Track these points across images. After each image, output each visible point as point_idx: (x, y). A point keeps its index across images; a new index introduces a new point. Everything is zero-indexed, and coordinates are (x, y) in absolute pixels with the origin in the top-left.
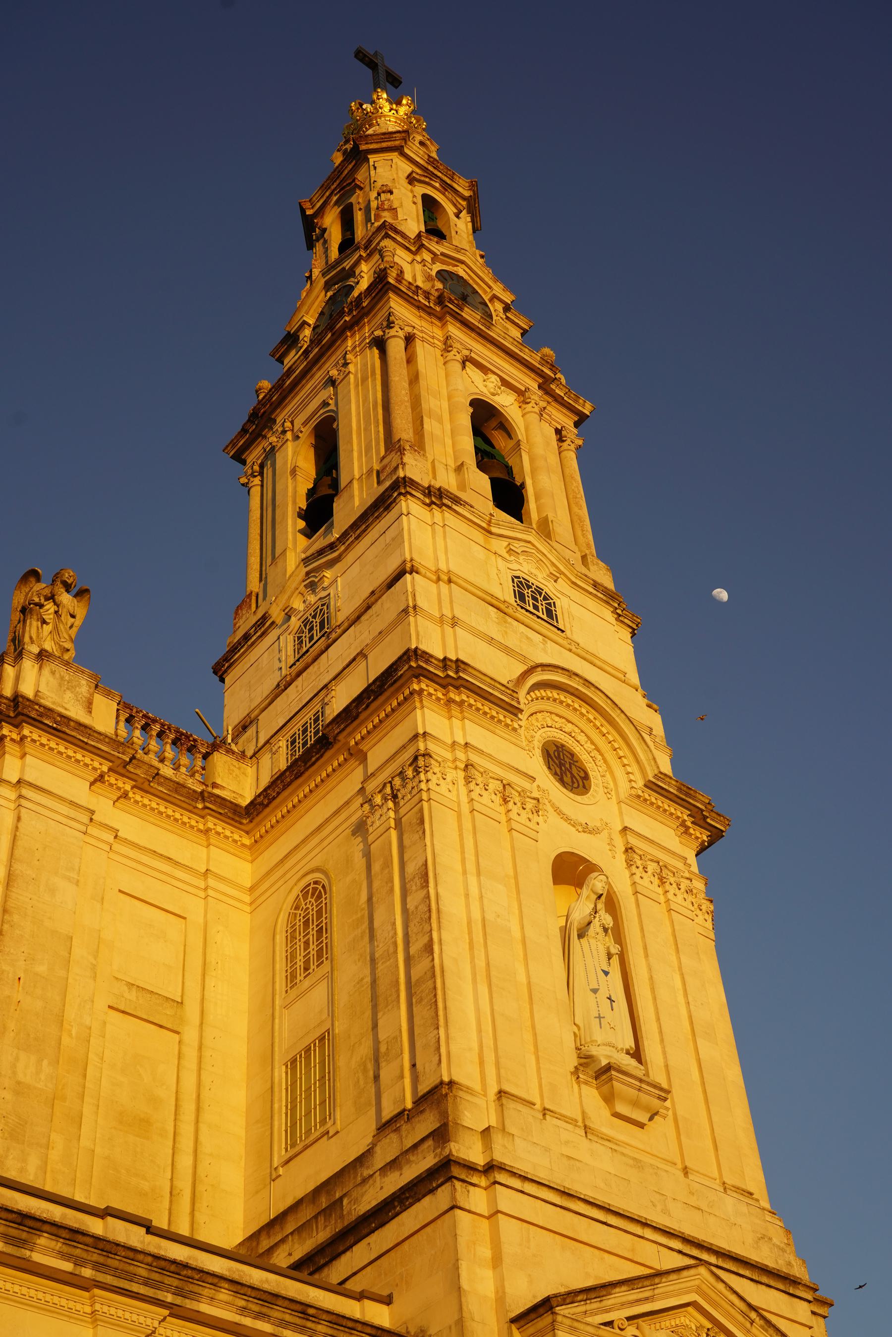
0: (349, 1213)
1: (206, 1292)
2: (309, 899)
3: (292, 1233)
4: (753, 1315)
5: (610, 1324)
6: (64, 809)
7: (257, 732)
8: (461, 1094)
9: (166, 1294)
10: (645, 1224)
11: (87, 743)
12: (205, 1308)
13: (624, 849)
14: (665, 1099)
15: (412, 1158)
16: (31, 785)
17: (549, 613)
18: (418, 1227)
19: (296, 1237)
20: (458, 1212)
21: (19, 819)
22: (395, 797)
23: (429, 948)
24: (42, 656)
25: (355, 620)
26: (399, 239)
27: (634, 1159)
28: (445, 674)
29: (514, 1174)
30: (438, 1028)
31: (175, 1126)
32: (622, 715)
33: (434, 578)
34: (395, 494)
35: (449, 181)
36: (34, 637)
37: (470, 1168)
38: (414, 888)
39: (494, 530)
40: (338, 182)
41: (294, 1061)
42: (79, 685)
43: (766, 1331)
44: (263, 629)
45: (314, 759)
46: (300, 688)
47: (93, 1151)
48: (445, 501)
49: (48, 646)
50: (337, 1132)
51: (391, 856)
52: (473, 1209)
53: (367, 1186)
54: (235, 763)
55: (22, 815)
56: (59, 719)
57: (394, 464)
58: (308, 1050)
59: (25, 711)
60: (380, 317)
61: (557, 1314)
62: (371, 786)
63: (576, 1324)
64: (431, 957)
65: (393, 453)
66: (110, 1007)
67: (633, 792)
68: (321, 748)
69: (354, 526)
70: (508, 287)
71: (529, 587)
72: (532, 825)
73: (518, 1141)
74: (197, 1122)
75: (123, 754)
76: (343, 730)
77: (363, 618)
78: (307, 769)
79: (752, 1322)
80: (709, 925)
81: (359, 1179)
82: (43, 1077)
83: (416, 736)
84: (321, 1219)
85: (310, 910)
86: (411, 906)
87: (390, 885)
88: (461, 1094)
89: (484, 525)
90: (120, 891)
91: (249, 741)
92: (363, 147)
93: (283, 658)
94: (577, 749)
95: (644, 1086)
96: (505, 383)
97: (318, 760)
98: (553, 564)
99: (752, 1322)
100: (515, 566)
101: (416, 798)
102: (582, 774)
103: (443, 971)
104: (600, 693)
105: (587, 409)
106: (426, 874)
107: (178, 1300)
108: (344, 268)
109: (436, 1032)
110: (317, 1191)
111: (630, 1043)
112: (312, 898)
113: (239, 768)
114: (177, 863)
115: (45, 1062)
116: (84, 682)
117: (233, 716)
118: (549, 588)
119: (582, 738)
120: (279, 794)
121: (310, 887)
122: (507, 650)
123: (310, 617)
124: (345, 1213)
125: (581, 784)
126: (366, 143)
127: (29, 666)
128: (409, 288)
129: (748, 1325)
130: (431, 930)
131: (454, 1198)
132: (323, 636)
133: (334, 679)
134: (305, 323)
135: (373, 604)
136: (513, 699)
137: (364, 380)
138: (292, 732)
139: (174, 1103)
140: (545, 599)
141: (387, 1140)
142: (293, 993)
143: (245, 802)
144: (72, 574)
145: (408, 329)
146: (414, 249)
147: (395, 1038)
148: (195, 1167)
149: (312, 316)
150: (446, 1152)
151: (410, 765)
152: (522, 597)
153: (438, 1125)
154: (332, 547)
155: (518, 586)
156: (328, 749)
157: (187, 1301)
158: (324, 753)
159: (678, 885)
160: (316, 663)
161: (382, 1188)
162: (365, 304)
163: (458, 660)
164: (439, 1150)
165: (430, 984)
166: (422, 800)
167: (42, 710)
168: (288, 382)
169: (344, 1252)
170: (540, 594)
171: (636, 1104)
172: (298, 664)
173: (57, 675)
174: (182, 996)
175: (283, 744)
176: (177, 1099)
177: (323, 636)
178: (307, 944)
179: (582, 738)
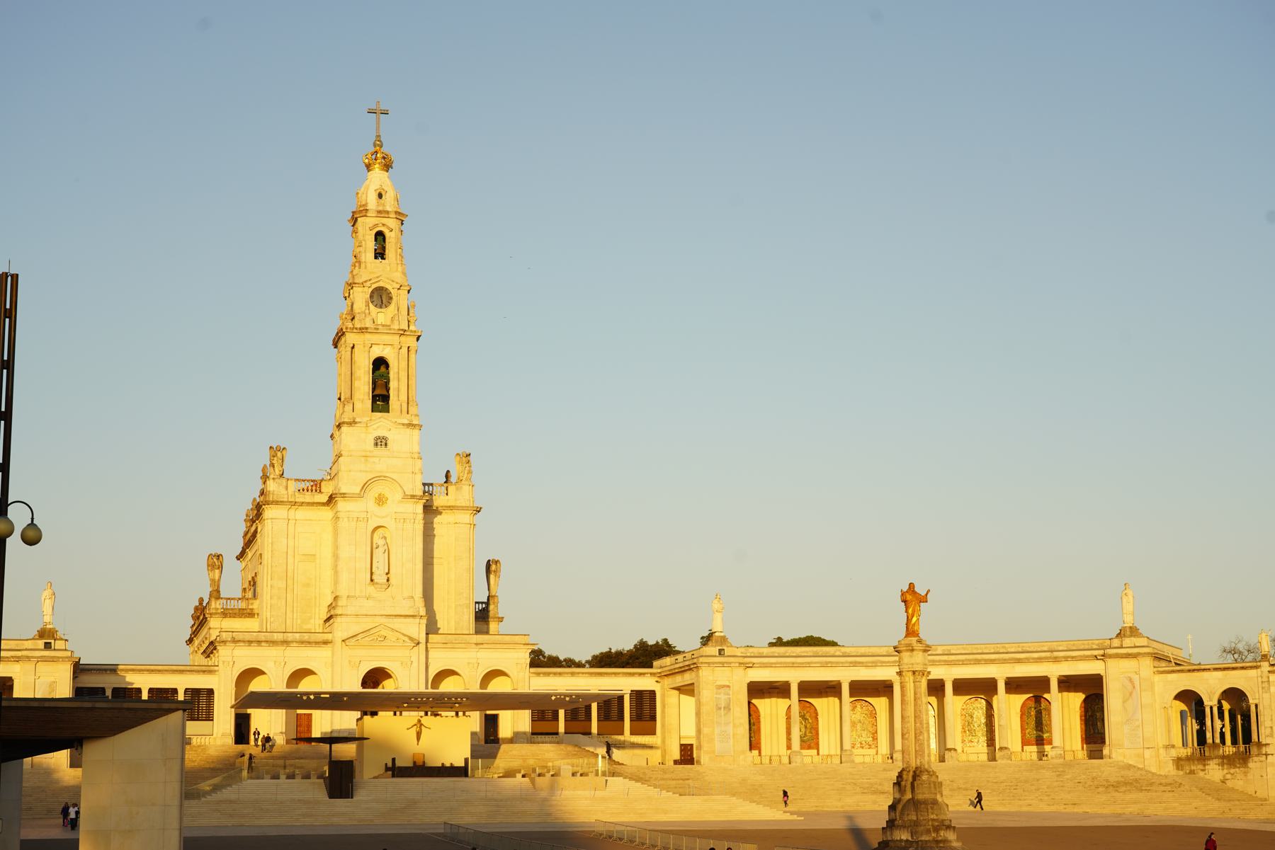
26: (357, 285)
37: (337, 615)
92: (355, 216)
111: (387, 571)
122: (366, 472)
127: (271, 481)
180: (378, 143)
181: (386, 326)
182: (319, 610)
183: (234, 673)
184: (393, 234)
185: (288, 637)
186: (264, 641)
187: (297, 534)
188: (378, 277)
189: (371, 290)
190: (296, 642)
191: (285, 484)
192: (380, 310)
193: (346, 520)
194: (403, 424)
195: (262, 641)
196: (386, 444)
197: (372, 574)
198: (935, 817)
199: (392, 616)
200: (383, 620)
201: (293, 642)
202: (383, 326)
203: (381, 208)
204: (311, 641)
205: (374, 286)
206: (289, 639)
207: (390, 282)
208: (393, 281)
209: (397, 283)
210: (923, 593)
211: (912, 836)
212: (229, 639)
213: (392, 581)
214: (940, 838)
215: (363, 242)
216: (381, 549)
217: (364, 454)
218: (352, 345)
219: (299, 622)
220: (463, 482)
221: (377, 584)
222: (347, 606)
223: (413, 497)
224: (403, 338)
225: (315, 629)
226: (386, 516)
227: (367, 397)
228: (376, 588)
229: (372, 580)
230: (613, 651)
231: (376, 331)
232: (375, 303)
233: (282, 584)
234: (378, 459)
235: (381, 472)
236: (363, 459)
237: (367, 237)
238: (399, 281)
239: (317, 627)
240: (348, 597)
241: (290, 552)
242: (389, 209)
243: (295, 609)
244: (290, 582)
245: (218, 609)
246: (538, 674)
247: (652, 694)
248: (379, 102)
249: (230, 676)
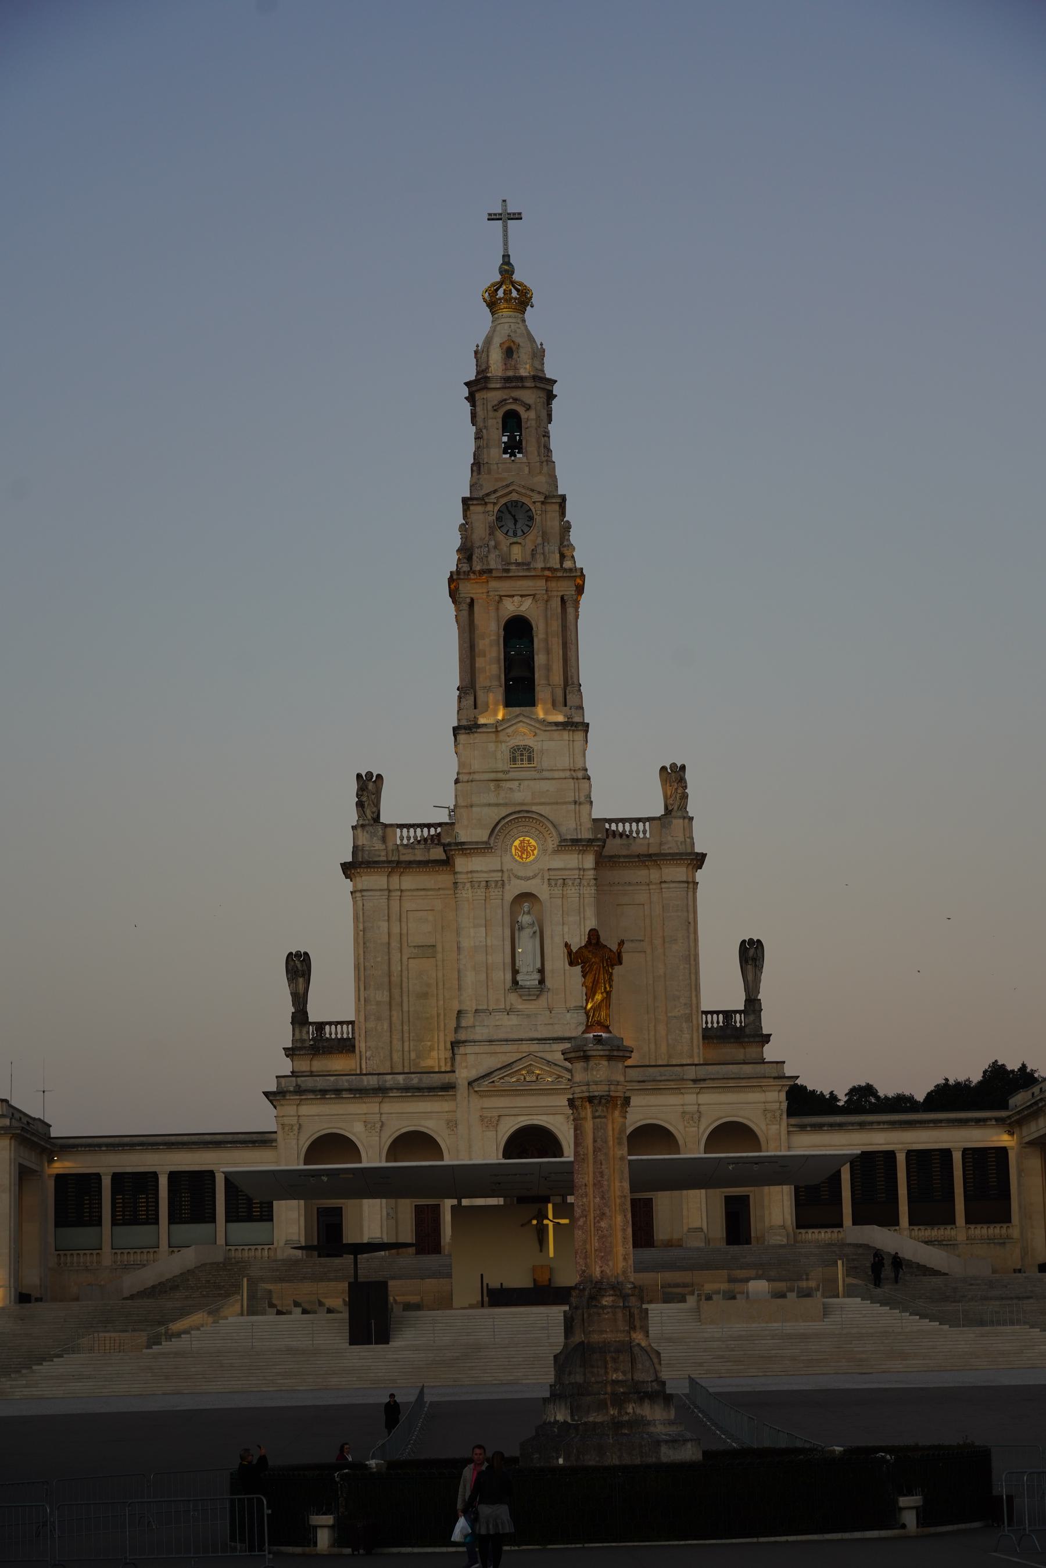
5: (493, 1082)
6: (378, 893)
12: (391, 1095)
16: (365, 890)
26: (475, 502)
39: (499, 729)
42: (378, 832)
55: (364, 903)
71: (519, 749)
73: (477, 1028)
82: (385, 996)
88: (462, 1015)
89: (494, 730)
95: (531, 990)
96: (522, 596)
111: (538, 965)
115: (385, 992)
118: (530, 741)
122: (497, 805)
125: (532, 854)
155: (513, 753)
171: (529, 995)
180: (507, 269)
181: (523, 564)
182: (445, 1035)
183: (301, 1143)
184: (532, 414)
185: (386, 1081)
186: (346, 1090)
187: (404, 915)
188: (508, 486)
189: (497, 508)
190: (398, 1089)
191: (380, 833)
192: (515, 540)
193: (468, 885)
194: (557, 724)
195: (342, 1090)
196: (530, 759)
197: (515, 972)
198: (621, 1377)
199: (549, 1039)
200: (534, 1047)
201: (391, 1089)
202: (518, 564)
203: (510, 373)
204: (423, 1085)
205: (503, 501)
206: (388, 1085)
207: (529, 493)
208: (533, 490)
209: (539, 493)
210: (614, 947)
211: (572, 1416)
212: (292, 1089)
213: (548, 983)
214: (626, 1418)
215: (484, 431)
216: (526, 933)
217: (493, 776)
218: (468, 600)
219: (413, 1055)
220: (674, 813)
221: (522, 987)
222: (474, 1026)
223: (575, 842)
224: (553, 585)
225: (440, 1067)
226: (534, 877)
227: (495, 683)
228: (521, 996)
229: (515, 982)
230: (951, 1082)
231: (505, 575)
232: (504, 530)
233: (382, 996)
234: (517, 783)
235: (522, 804)
236: (492, 785)
237: (490, 422)
238: (543, 490)
239: (442, 1063)
240: (476, 1011)
241: (395, 944)
242: (523, 373)
243: (406, 1035)
244: (396, 992)
245: (305, 1040)
246: (802, 1128)
247: (1002, 1152)
248: (504, 201)
249: (295, 1147)
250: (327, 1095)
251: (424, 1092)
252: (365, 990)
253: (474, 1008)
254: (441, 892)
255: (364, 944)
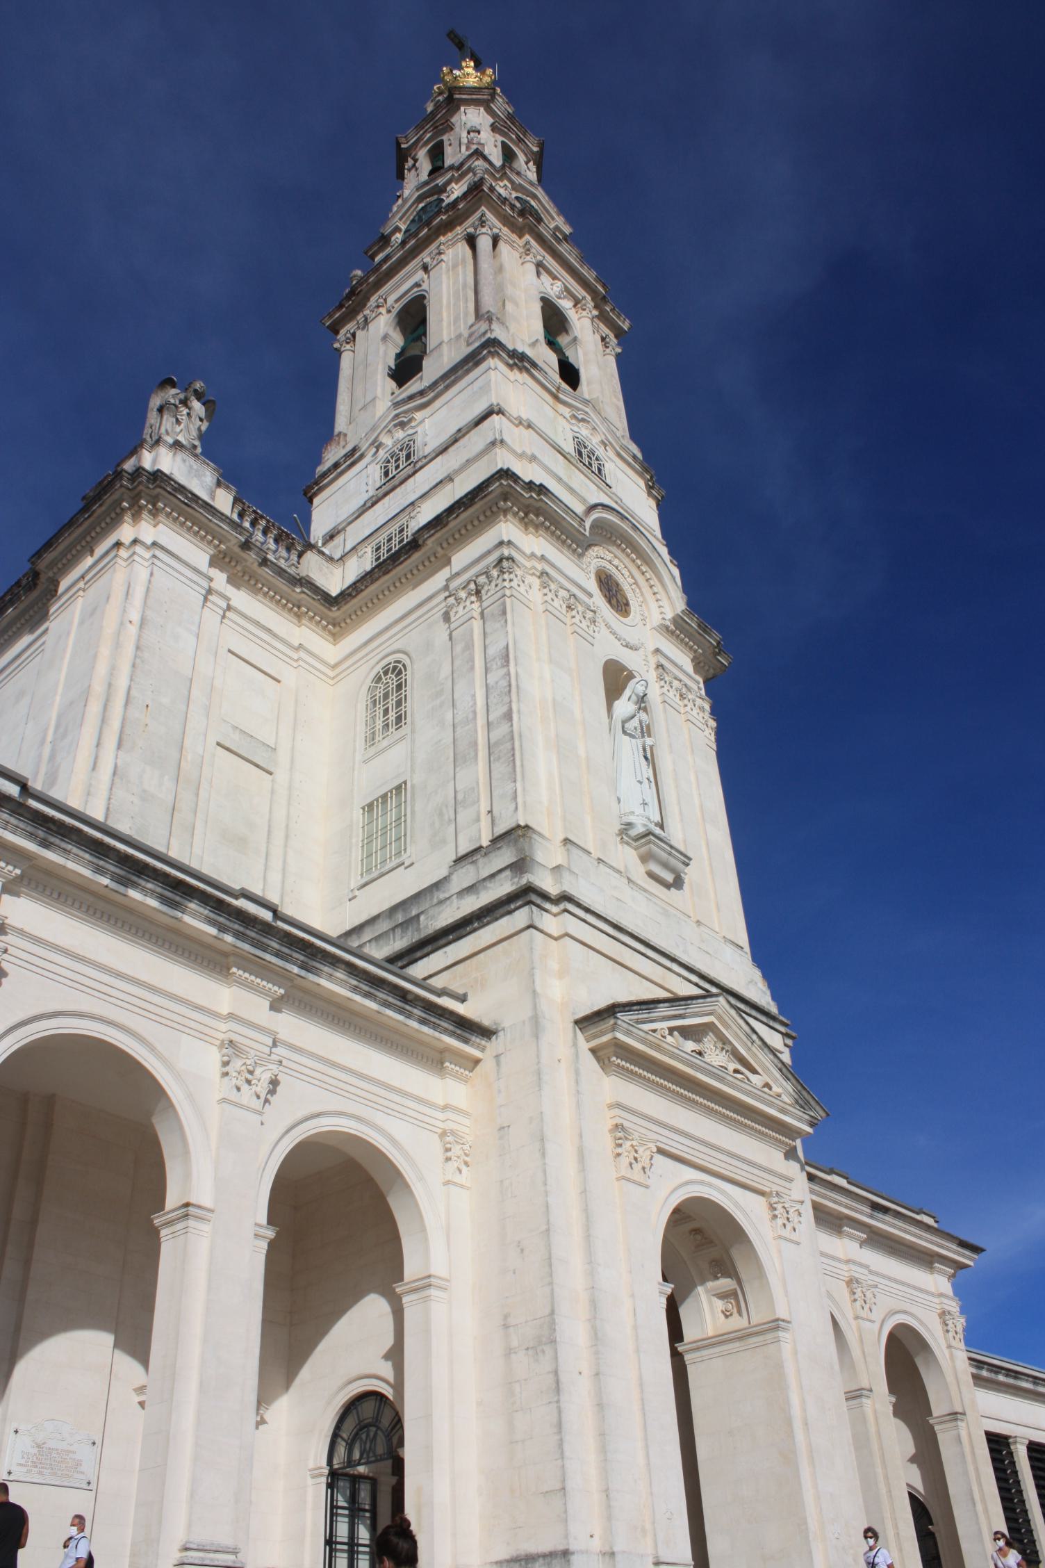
0: (426, 927)
1: (326, 969)
2: (390, 675)
3: (370, 941)
4: (754, 1037)
5: (654, 1031)
7: (345, 540)
8: (535, 836)
9: (293, 966)
10: (673, 960)
11: (211, 521)
13: (655, 666)
14: (687, 865)
15: (489, 885)
17: (599, 470)
18: (495, 940)
19: (373, 944)
20: (532, 930)
21: (152, 574)
22: (478, 592)
23: (508, 716)
24: (177, 445)
25: (443, 450)
27: (663, 909)
28: (529, 495)
29: (579, 905)
30: (515, 781)
31: (267, 847)
32: (660, 559)
33: (517, 422)
34: (485, 352)
35: (522, 136)
36: (170, 430)
37: (545, 896)
38: (495, 667)
40: (431, 123)
41: (370, 806)
42: (204, 475)
43: (763, 1050)
44: (352, 459)
45: (402, 559)
46: (387, 505)
47: (202, 858)
48: (526, 364)
49: (181, 438)
50: (412, 864)
51: (473, 640)
52: (546, 930)
53: (445, 906)
54: (325, 563)
55: (155, 572)
56: (190, 495)
57: (482, 330)
58: (384, 797)
59: (163, 485)
60: (474, 218)
61: (618, 1018)
62: (454, 585)
63: (631, 1028)
64: (509, 724)
65: (482, 322)
66: (218, 744)
67: (663, 622)
68: (410, 550)
69: (444, 377)
70: (569, 220)
71: (585, 447)
72: (591, 632)
74: (286, 846)
75: (240, 534)
76: (433, 535)
77: (451, 450)
78: (395, 567)
79: (753, 1042)
80: (713, 738)
81: (435, 901)
83: (501, 543)
84: (398, 931)
85: (390, 684)
86: (491, 681)
87: (470, 663)
89: (554, 391)
90: (230, 651)
91: (336, 547)
93: (370, 483)
94: (621, 580)
95: (673, 851)
97: (405, 560)
98: (604, 434)
99: (753, 1042)
100: (576, 429)
101: (499, 594)
102: (625, 602)
103: (520, 736)
104: (644, 538)
105: (626, 326)
106: (507, 656)
107: (303, 973)
108: (437, 185)
109: (513, 784)
110: (393, 910)
111: (657, 818)
112: (392, 673)
113: (328, 568)
114: (275, 636)
115: (166, 777)
116: (208, 473)
117: (318, 531)
118: (600, 451)
119: (625, 572)
120: (366, 587)
121: (391, 666)
123: (397, 451)
124: (421, 926)
126: (460, 94)
128: (499, 198)
129: (750, 1044)
130: (511, 702)
131: (531, 918)
132: (410, 464)
133: (421, 497)
134: (397, 229)
135: (460, 438)
136: (581, 525)
137: (455, 266)
138: (377, 541)
139: (266, 829)
140: (597, 459)
141: (464, 870)
142: (372, 751)
143: (334, 594)
144: (202, 385)
145: (495, 231)
146: (498, 176)
147: (473, 788)
148: (283, 882)
149: (404, 223)
150: (524, 881)
151: (495, 567)
152: (580, 454)
153: (515, 860)
154: (422, 393)
156: (416, 551)
157: (310, 974)
158: (412, 554)
159: (694, 701)
160: (403, 486)
161: (458, 908)
162: (460, 207)
163: (541, 485)
164: (516, 880)
165: (508, 745)
166: (505, 595)
167: (176, 486)
168: (384, 268)
169: (421, 958)
170: (594, 455)
171: (665, 866)
172: (384, 487)
173: (187, 463)
174: (276, 743)
175: (369, 550)
176: (269, 826)
177: (410, 464)
178: (386, 712)
179: (625, 572)
193: (536, 582)
228: (644, 859)
250: (135, 885)
251: (409, 1015)
252: (120, 745)
253: (562, 837)
254: (302, 654)
255: (138, 648)
